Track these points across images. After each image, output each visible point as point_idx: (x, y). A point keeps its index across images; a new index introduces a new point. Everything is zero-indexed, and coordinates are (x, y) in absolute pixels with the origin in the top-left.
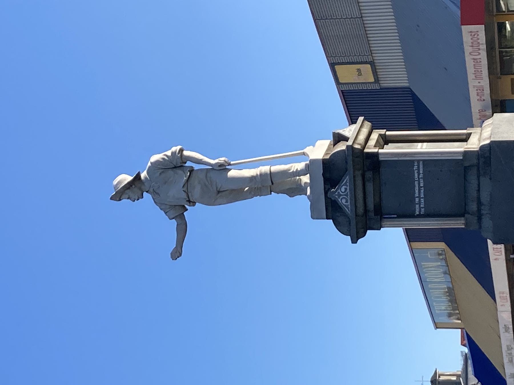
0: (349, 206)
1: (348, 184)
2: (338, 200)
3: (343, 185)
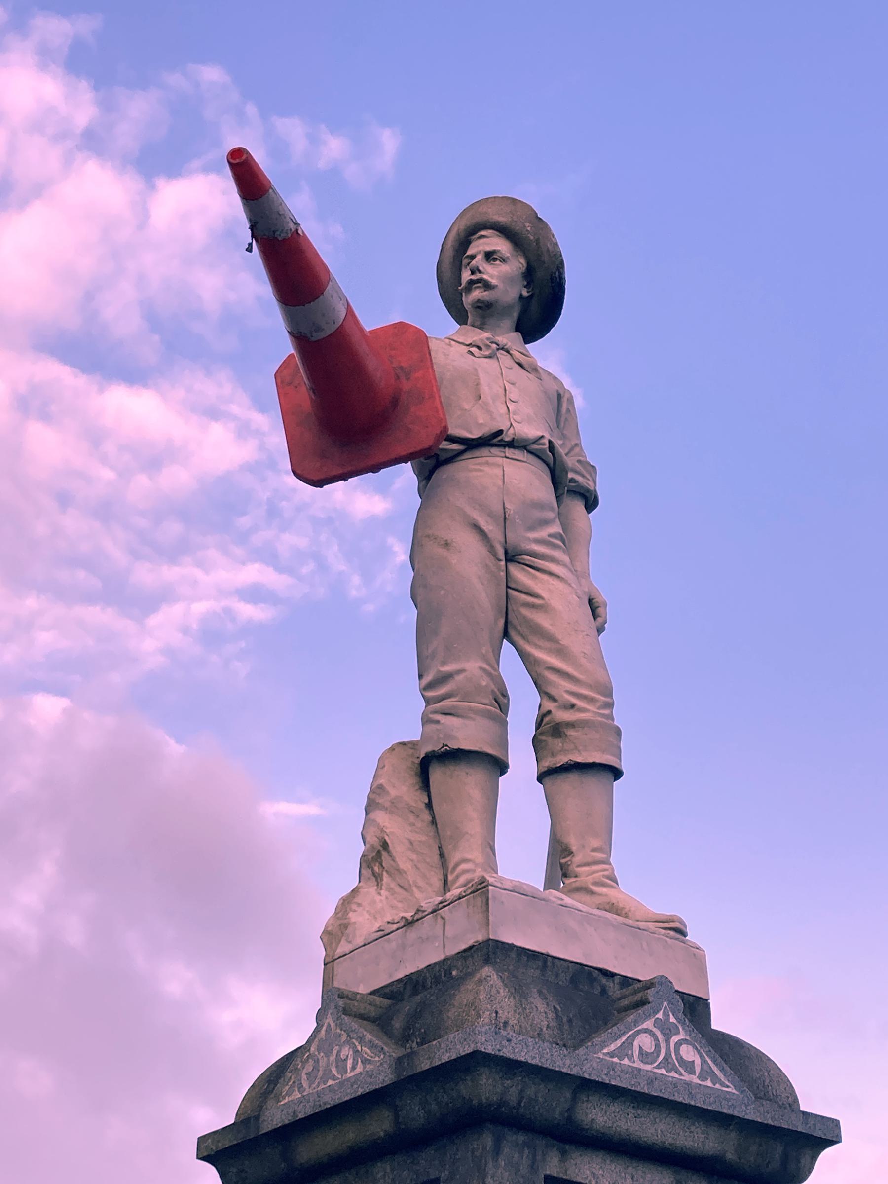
1: (709, 1083)
2: (647, 1017)
3: (704, 1061)
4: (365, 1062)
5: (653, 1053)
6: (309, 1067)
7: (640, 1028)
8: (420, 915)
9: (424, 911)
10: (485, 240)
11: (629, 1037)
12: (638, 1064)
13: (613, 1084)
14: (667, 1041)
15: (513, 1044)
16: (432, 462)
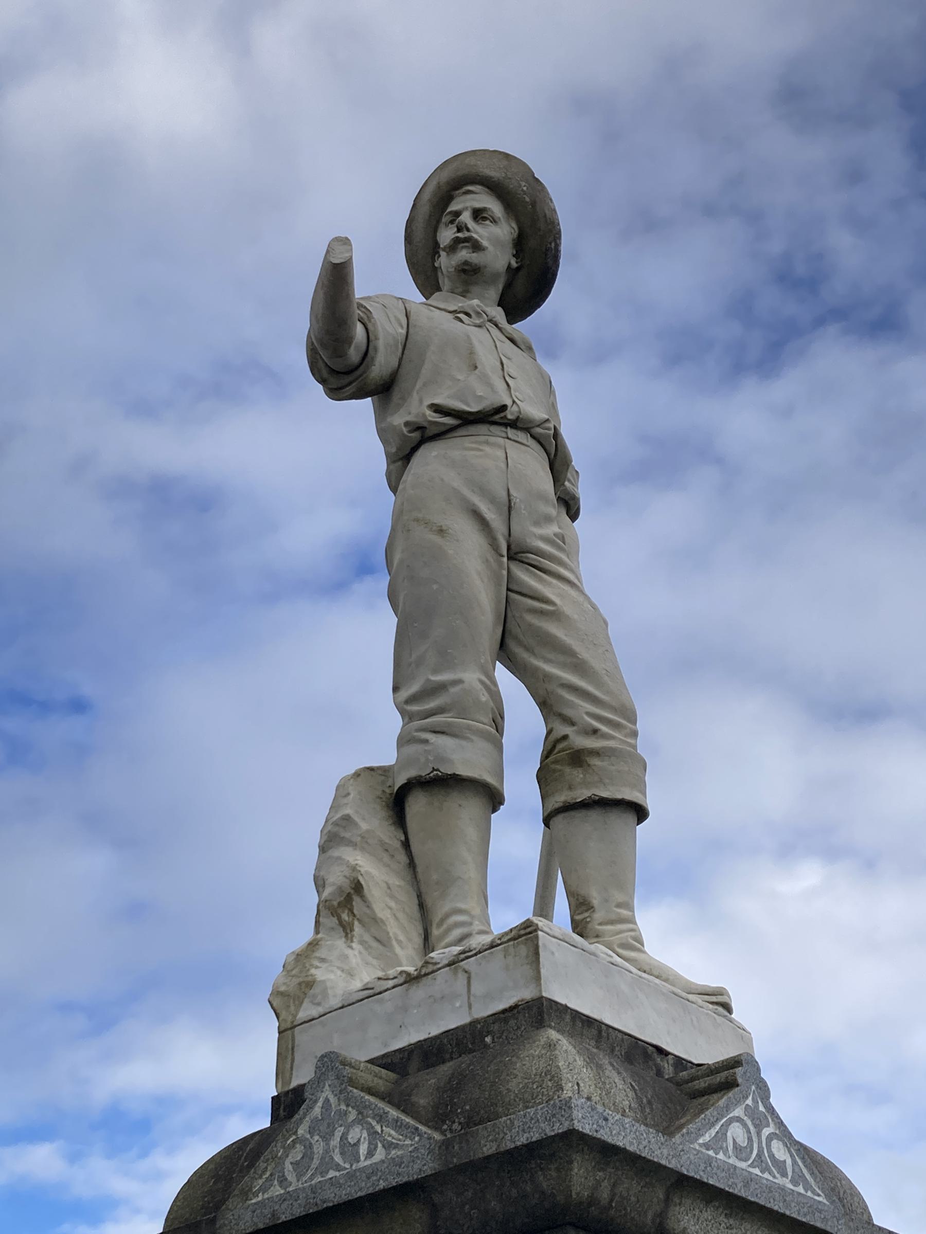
1: (801, 1189)
2: (738, 1103)
3: (794, 1162)
4: (388, 1146)
5: (746, 1147)
6: (297, 1154)
7: (731, 1115)
8: (430, 968)
9: (436, 964)
10: (469, 196)
11: (722, 1125)
12: (733, 1161)
13: (711, 1183)
14: (759, 1134)
15: (610, 1125)
16: (416, 435)
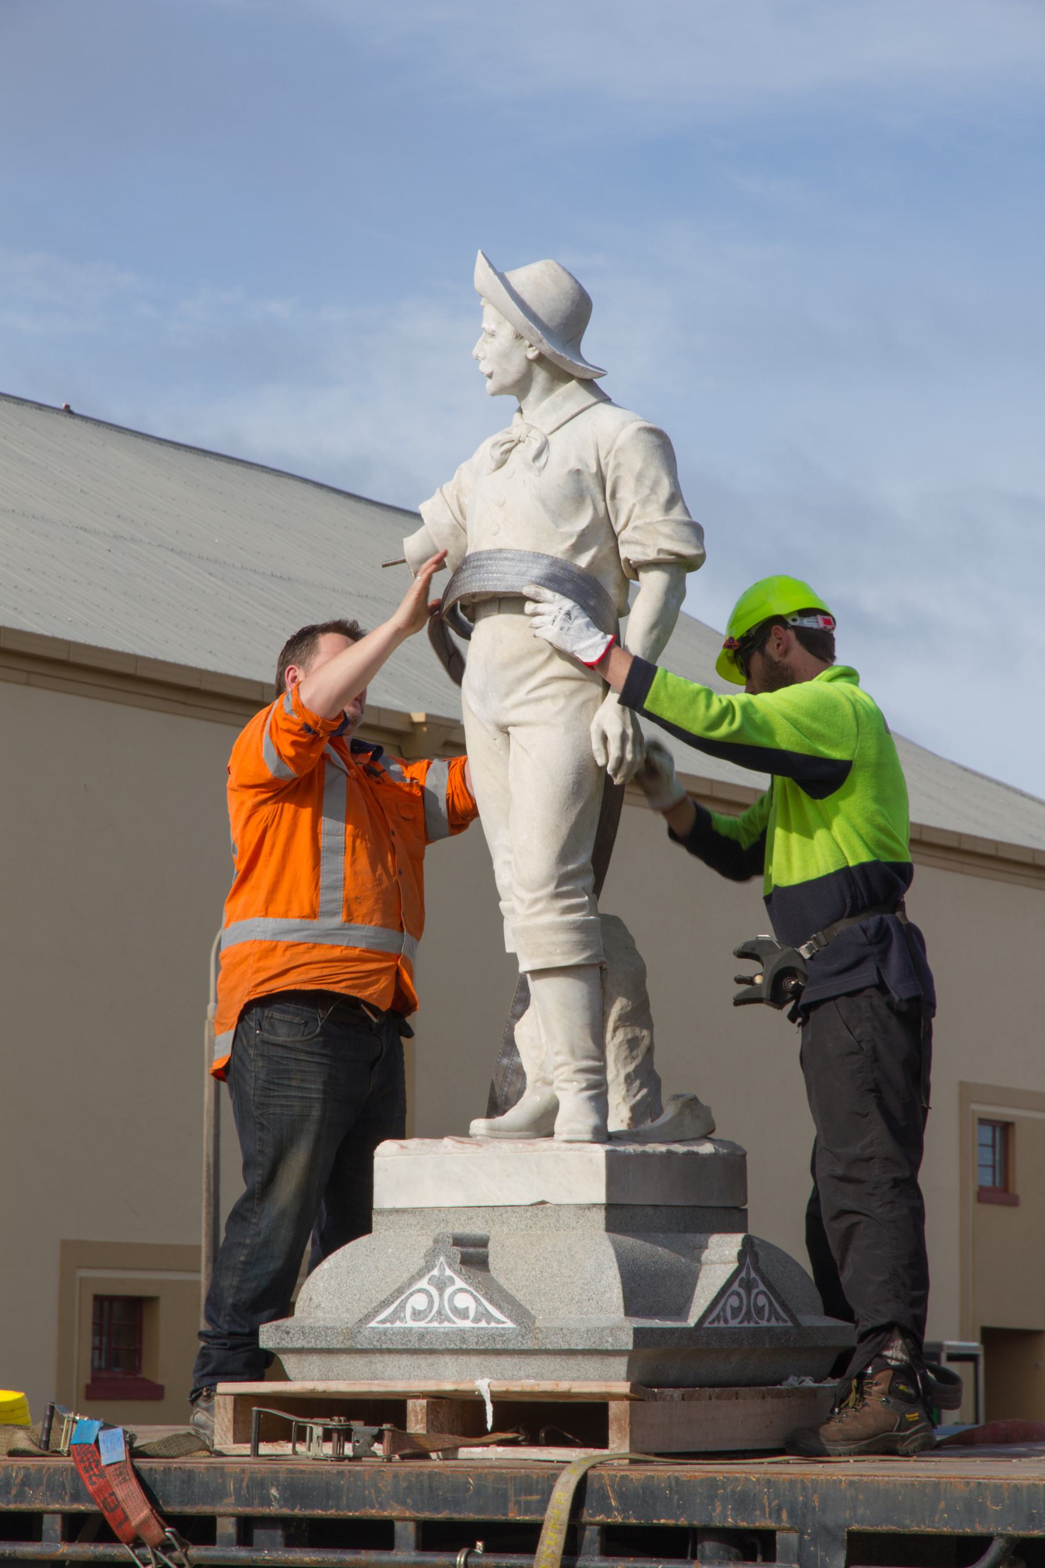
0: (398, 1324)
1: (483, 1324)
5: (426, 1310)
12: (410, 1323)
14: (441, 1295)
15: (291, 1335)
